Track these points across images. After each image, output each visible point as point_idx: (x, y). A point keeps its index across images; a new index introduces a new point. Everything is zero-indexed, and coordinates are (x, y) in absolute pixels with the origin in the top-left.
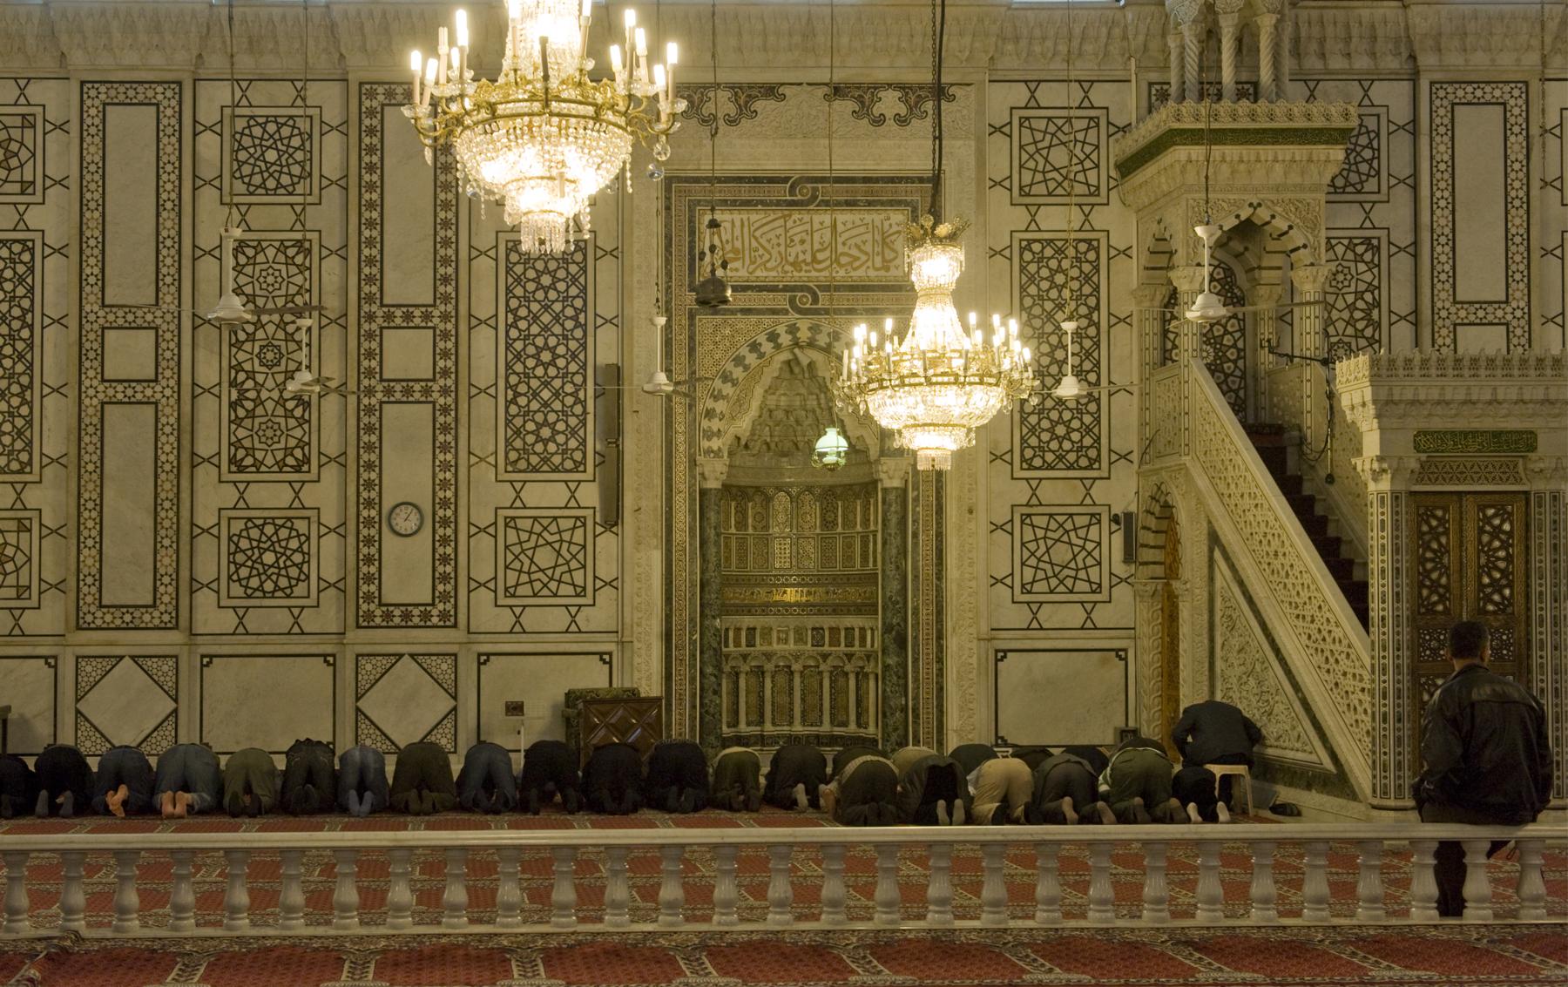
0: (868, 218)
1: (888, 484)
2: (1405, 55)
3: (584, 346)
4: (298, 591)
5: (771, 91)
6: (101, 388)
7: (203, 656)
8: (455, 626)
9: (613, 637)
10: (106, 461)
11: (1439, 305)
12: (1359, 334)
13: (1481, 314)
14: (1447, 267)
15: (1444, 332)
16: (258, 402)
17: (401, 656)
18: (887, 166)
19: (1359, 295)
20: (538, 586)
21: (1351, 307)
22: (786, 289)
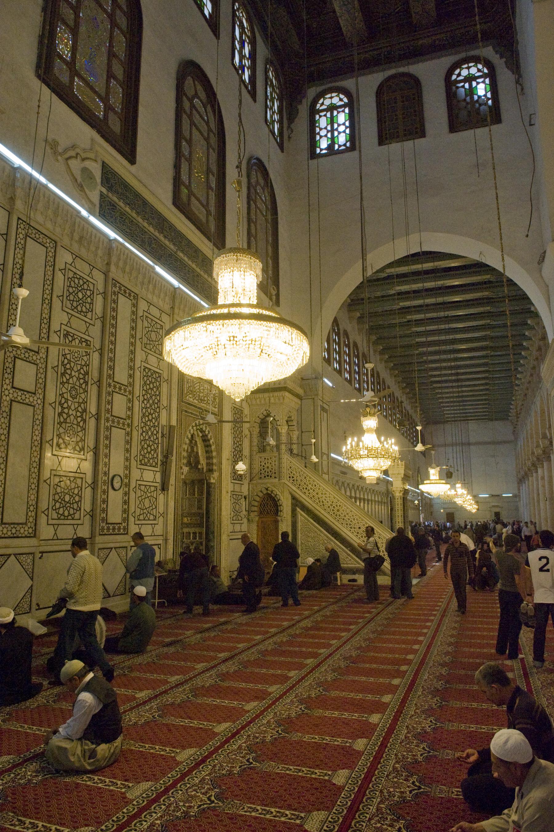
1: (212, 481)
3: (159, 415)
4: (77, 516)
6: (11, 391)
7: (40, 552)
8: (127, 534)
9: (161, 538)
10: (11, 434)
16: (69, 415)
17: (112, 548)
20: (145, 515)
22: (199, 408)
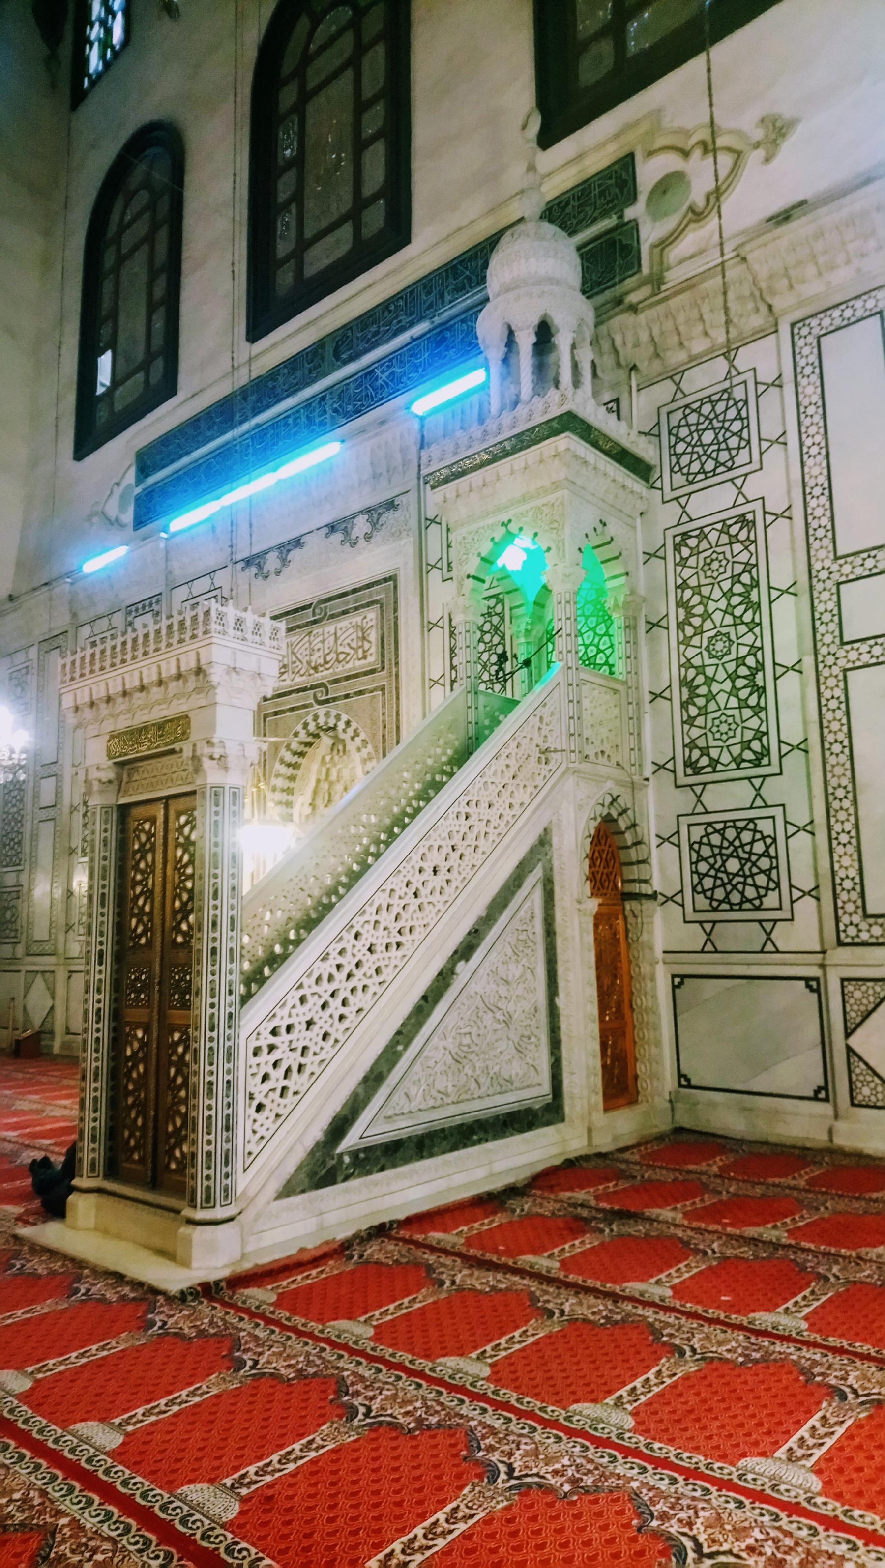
0: (354, 620)
2: (764, 309)
5: (297, 543)
11: (817, 566)
12: (738, 621)
13: (870, 563)
14: (825, 521)
15: (825, 596)
18: (365, 578)
19: (736, 579)
21: (728, 594)
